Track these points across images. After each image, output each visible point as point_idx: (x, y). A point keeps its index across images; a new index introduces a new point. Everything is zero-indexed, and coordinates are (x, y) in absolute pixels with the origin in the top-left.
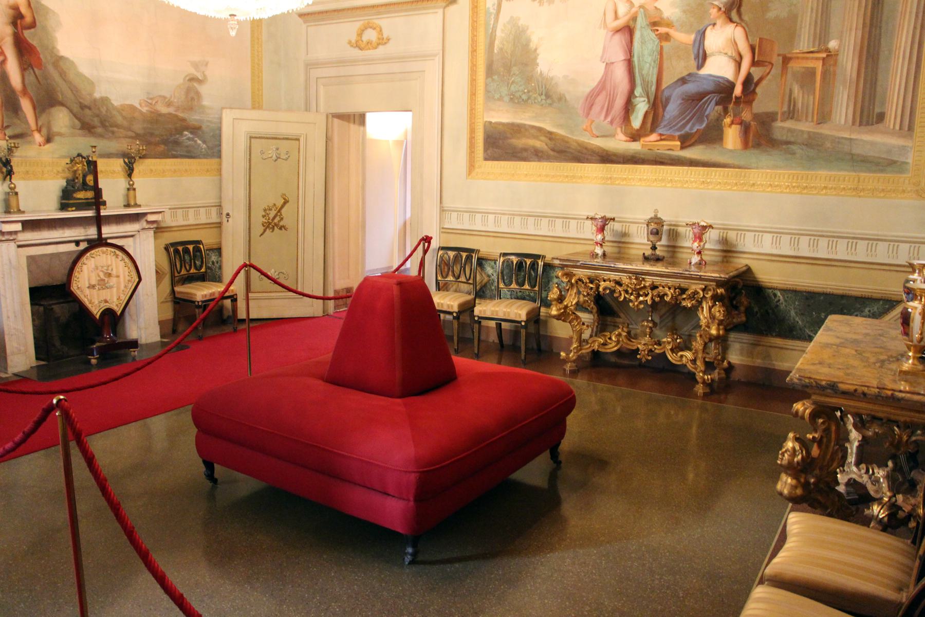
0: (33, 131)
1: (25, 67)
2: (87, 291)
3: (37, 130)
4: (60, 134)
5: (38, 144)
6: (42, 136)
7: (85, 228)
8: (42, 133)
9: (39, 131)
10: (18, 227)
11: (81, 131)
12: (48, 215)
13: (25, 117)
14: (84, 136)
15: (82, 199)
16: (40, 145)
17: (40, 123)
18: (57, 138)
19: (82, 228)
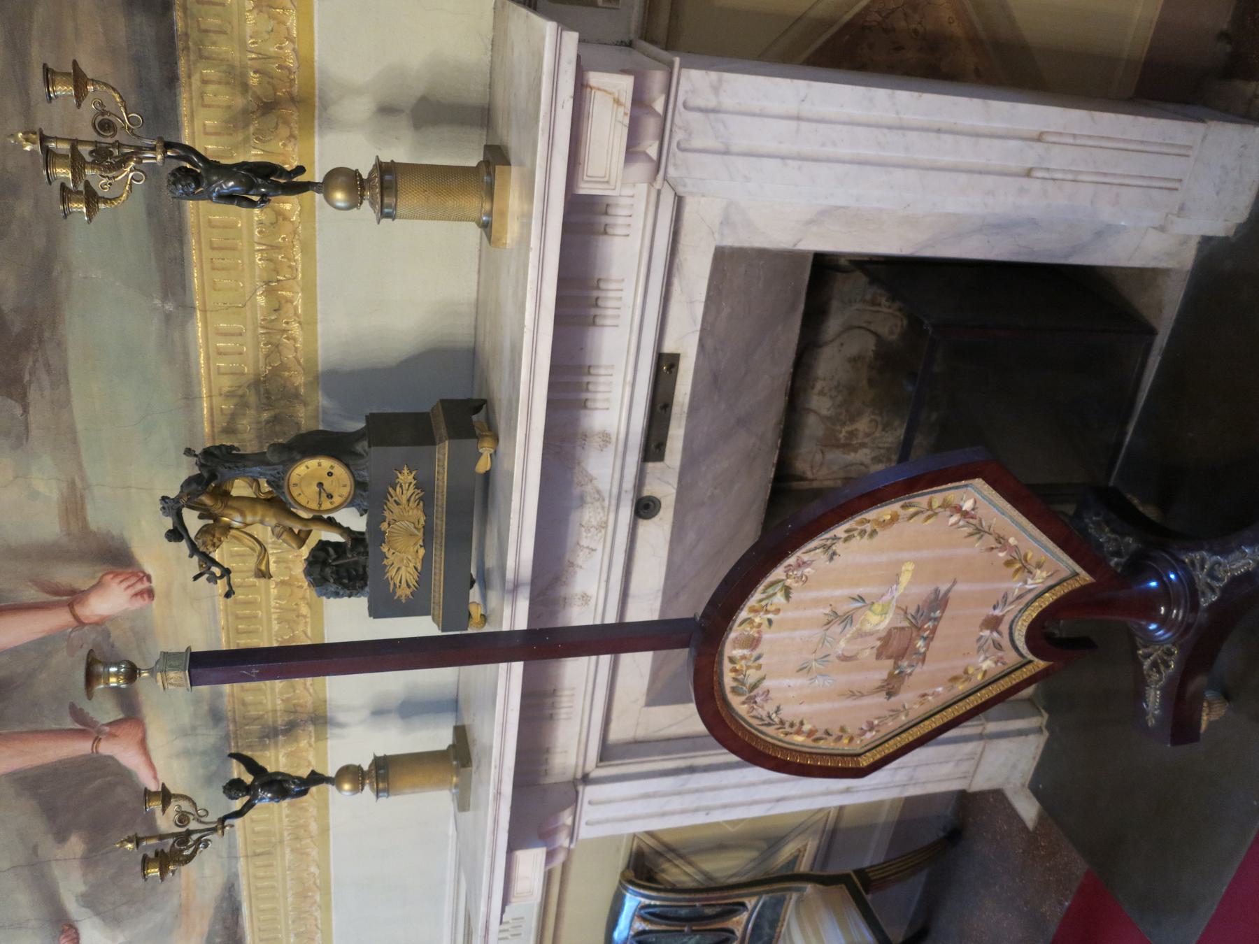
0: (80, 623)
2: (907, 697)
3: (71, 606)
4: (74, 505)
5: (139, 603)
6: (99, 585)
7: (582, 501)
8: (82, 583)
9: (73, 597)
10: (531, 862)
11: (33, 395)
12: (498, 794)
14: (60, 377)
15: (427, 560)
16: (150, 593)
17: (32, 594)
18: (100, 517)
19: (574, 516)
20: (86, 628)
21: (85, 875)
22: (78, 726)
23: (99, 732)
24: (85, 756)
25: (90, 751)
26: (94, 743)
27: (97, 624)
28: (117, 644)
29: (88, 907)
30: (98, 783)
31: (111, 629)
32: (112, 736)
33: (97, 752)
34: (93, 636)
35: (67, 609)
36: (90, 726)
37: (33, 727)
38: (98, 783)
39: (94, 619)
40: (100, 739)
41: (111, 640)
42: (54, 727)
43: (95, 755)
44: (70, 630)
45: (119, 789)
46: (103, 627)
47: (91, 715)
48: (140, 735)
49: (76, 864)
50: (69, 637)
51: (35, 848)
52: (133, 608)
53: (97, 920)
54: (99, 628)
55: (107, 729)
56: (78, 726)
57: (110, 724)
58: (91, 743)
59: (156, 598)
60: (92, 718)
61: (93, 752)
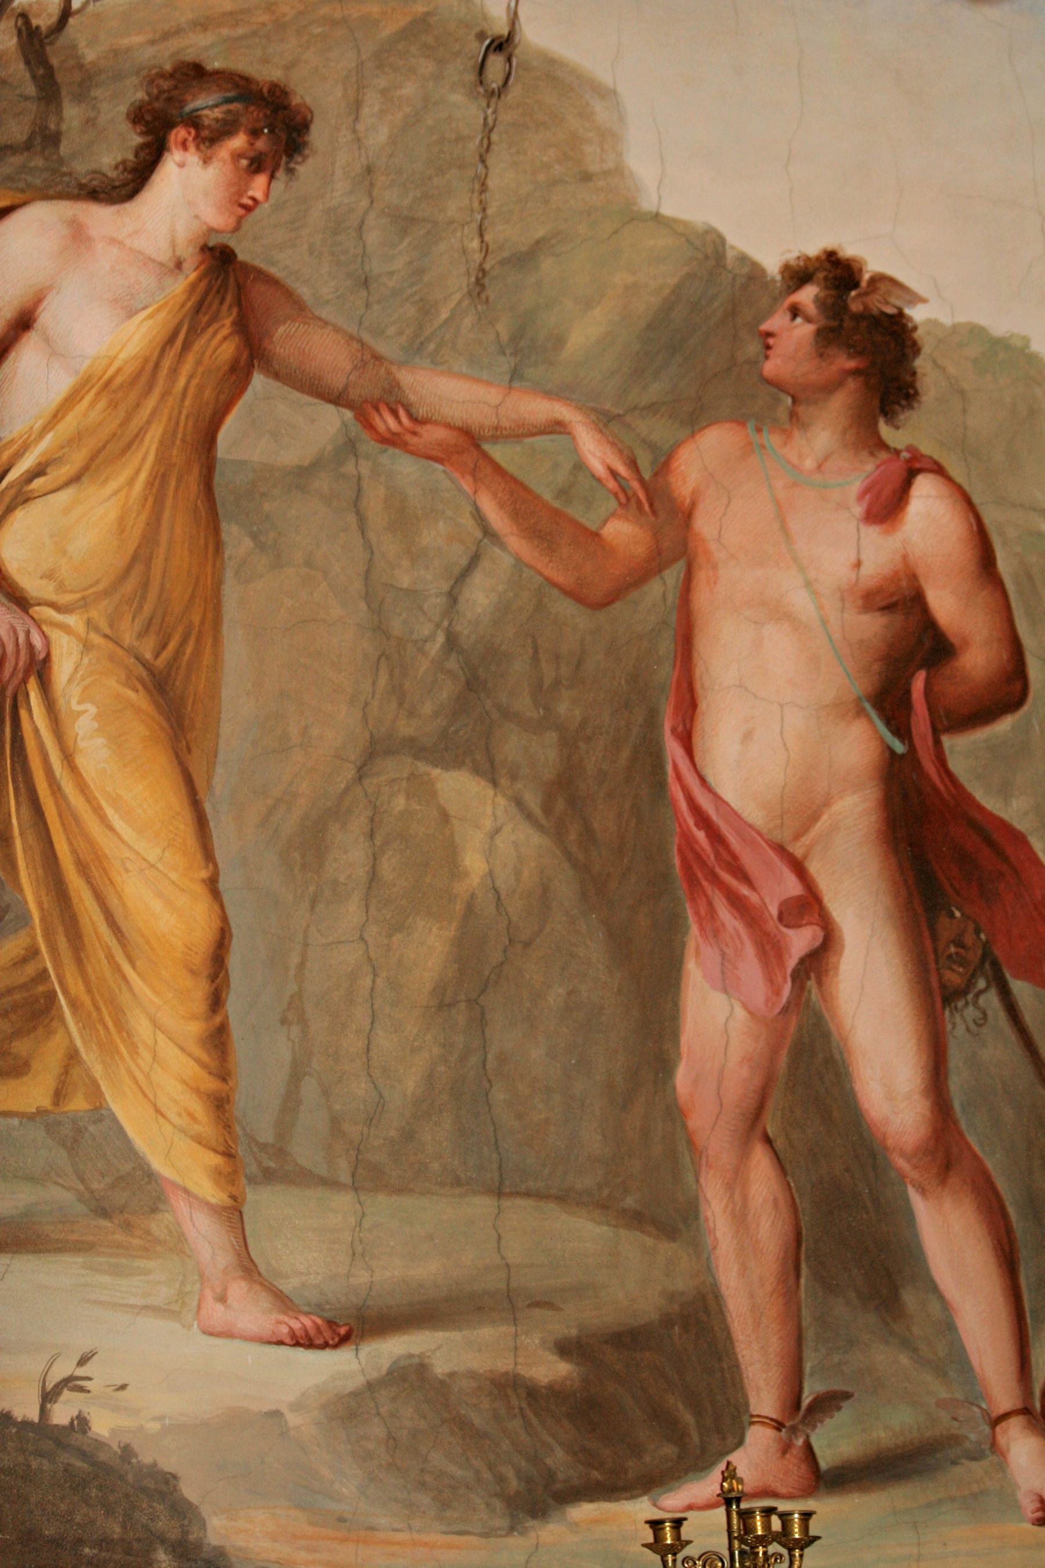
1: (954, 977)
3: (1025, 1411)
13: (948, 1326)
20: (987, 1429)
21: (472, 1375)
22: (806, 1400)
23: (794, 1430)
24: (747, 1405)
25: (754, 1413)
26: (772, 1419)
27: (993, 1443)
28: (958, 1470)
29: (390, 1373)
30: (688, 1418)
31: (985, 1463)
32: (786, 1448)
33: (752, 1423)
34: (973, 1437)
35: (1019, 1405)
36: (805, 1417)
37: (810, 1334)
38: (688, 1418)
39: (1001, 1440)
40: (779, 1430)
41: (964, 1461)
42: (808, 1367)
43: (745, 1418)
44: (984, 1406)
45: (670, 1450)
46: (988, 1452)
47: (828, 1421)
48: (783, 1490)
49: (504, 1364)
50: (972, 1404)
51: (548, 1305)
52: (1020, 1495)
53: (357, 1382)
54: (986, 1447)
55: (800, 1442)
56: (806, 1400)
57: (809, 1448)
58: (774, 1416)
59: (1036, 1528)
60: (822, 1422)
61: (752, 1416)
